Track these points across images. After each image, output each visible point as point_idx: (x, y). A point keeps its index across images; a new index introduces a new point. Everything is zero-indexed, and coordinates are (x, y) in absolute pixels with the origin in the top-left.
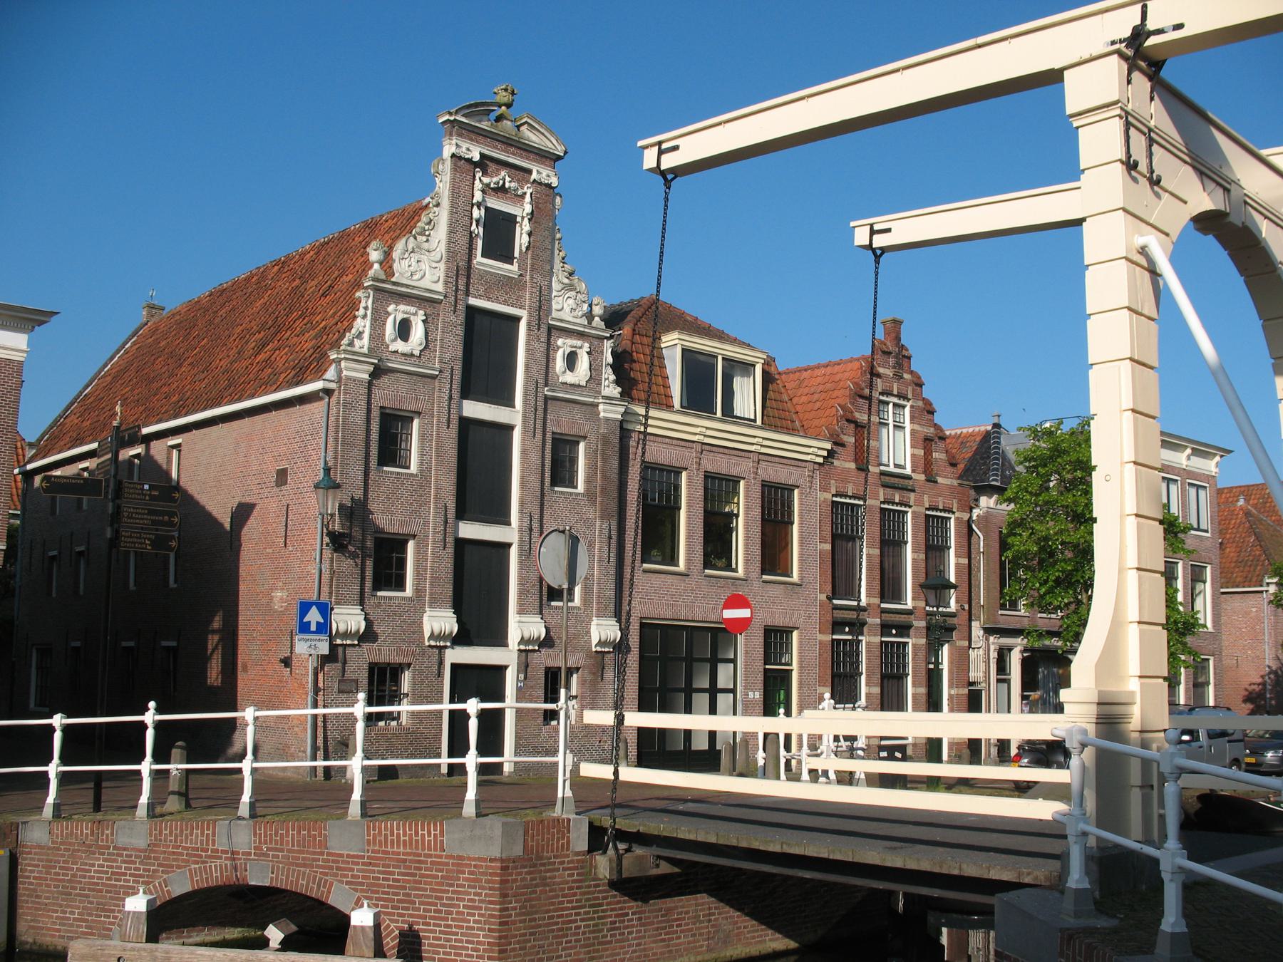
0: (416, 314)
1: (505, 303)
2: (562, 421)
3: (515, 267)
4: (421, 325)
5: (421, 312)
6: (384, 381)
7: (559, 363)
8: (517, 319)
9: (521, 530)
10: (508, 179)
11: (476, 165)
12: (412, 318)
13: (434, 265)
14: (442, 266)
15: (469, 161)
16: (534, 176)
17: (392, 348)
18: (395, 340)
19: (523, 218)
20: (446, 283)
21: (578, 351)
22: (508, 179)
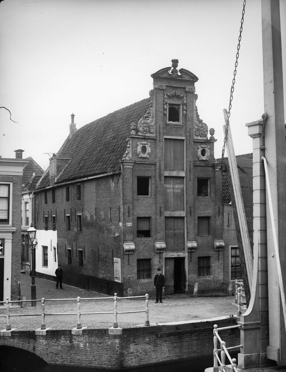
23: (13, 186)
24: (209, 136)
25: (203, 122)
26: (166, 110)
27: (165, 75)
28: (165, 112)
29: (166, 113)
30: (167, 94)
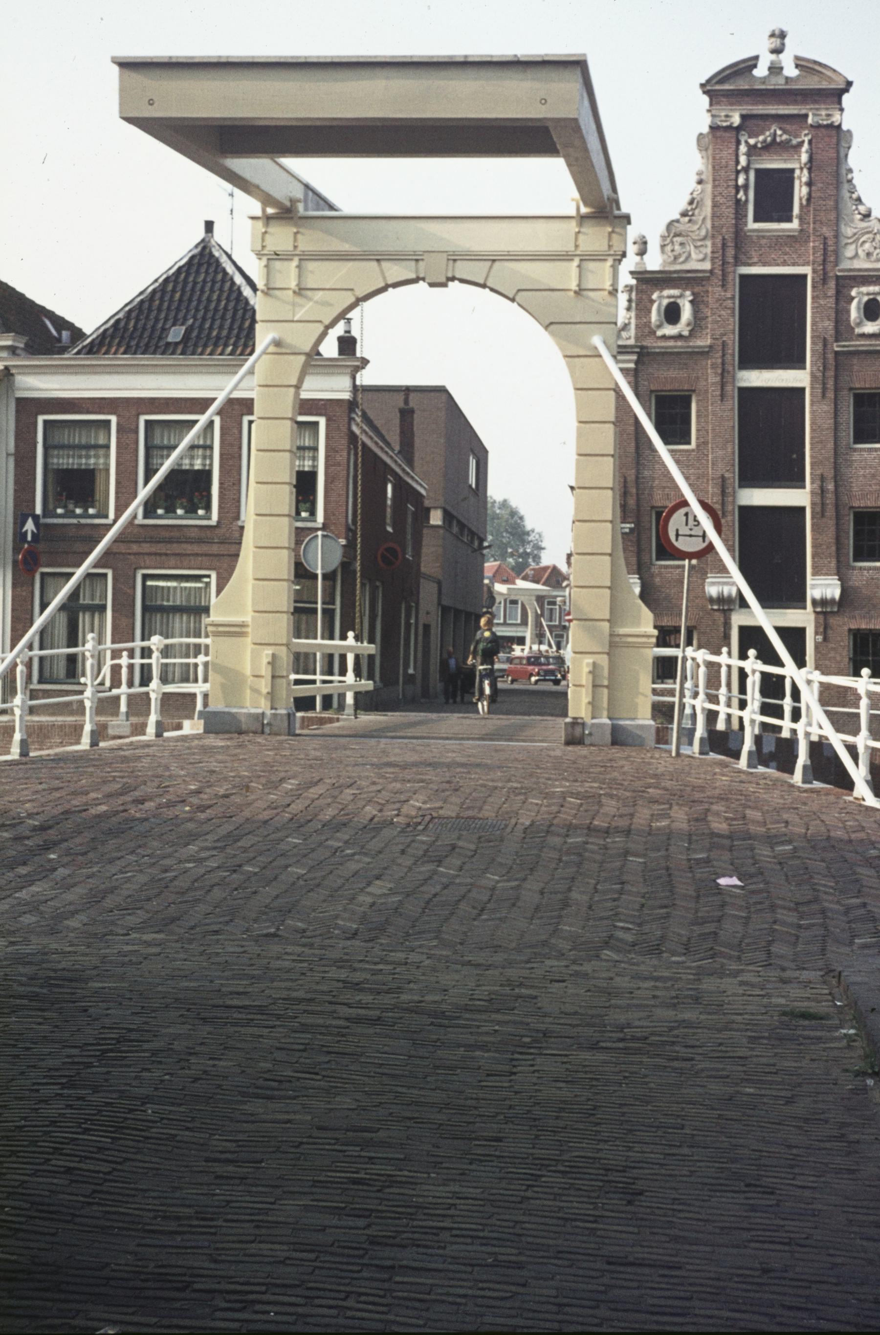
0: (681, 296)
1: (785, 264)
3: (795, 224)
5: (688, 293)
8: (805, 276)
9: (813, 493)
10: (779, 132)
11: (738, 129)
12: (679, 301)
13: (699, 243)
14: (709, 243)
15: (730, 128)
16: (810, 120)
17: (659, 333)
19: (801, 169)
20: (713, 259)
22: (779, 132)
23: (328, 426)
28: (741, 195)
29: (743, 198)
30: (746, 142)
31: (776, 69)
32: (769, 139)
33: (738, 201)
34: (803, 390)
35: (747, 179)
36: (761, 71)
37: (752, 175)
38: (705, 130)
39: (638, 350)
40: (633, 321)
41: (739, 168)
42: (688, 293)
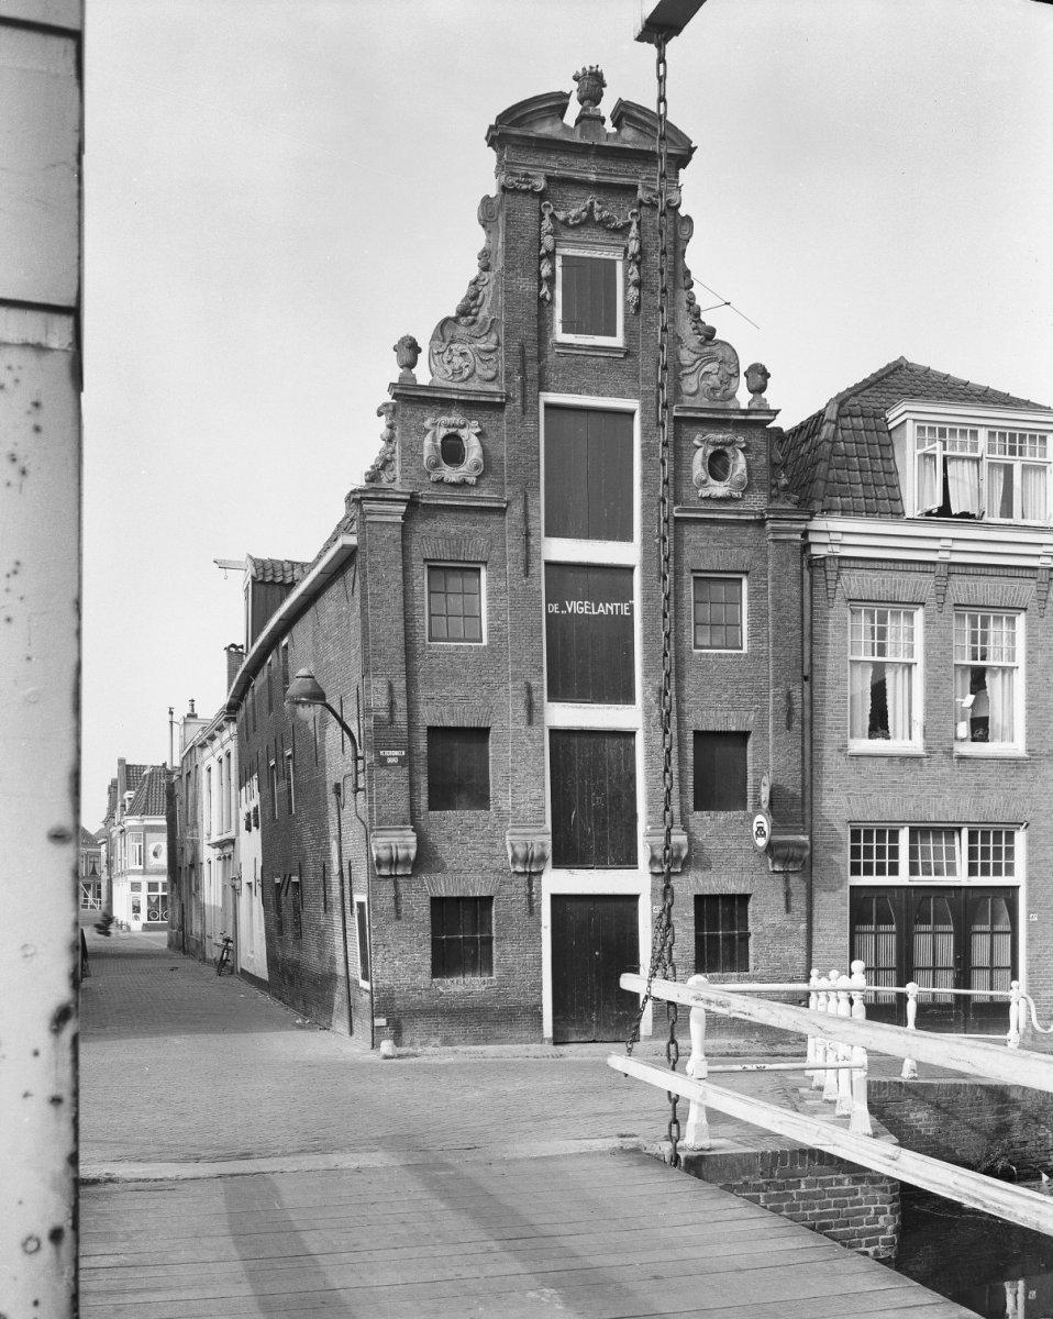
2: (702, 550)
4: (474, 441)
6: (422, 527)
7: (698, 469)
8: (631, 414)
10: (597, 206)
11: (542, 196)
15: (530, 192)
16: (641, 194)
18: (436, 465)
21: (728, 450)
24: (743, 398)
25: (717, 337)
26: (552, 289)
27: (546, 129)
30: (552, 216)
31: (589, 120)
32: (585, 214)
33: (541, 300)
34: (630, 569)
35: (553, 270)
36: (570, 118)
37: (559, 261)
38: (493, 191)
39: (408, 497)
40: (397, 456)
41: (543, 251)
42: (475, 423)
